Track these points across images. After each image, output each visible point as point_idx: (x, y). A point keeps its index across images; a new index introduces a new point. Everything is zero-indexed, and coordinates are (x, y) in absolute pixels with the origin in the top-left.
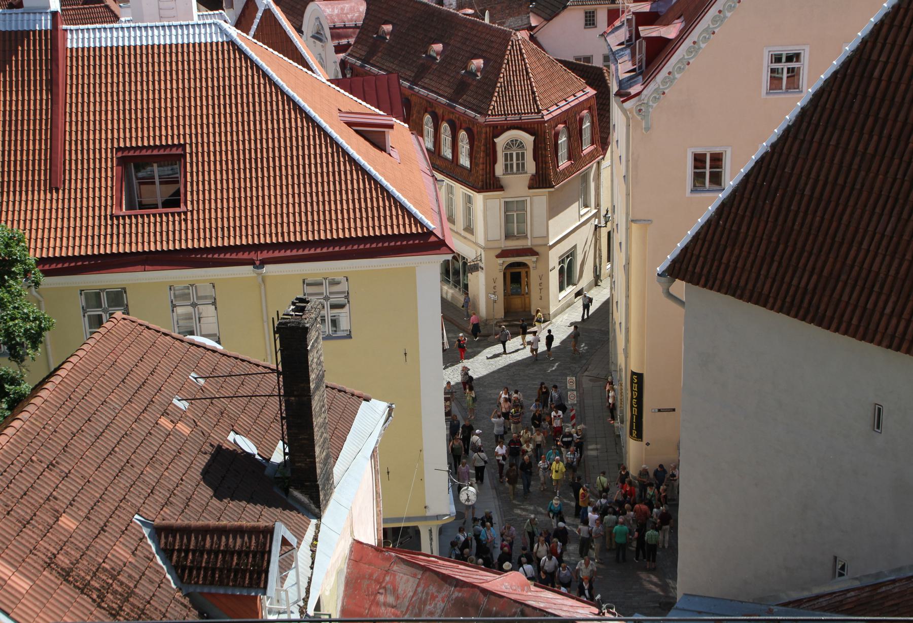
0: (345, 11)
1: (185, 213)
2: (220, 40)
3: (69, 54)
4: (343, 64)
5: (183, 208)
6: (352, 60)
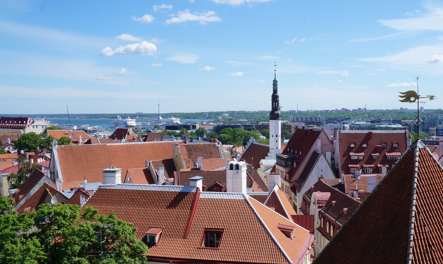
0: (323, 196)
1: (219, 250)
2: (243, 199)
3: (199, 200)
4: (320, 212)
5: (218, 248)
6: (322, 211)
